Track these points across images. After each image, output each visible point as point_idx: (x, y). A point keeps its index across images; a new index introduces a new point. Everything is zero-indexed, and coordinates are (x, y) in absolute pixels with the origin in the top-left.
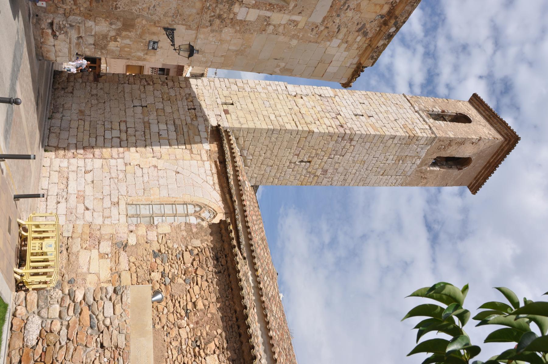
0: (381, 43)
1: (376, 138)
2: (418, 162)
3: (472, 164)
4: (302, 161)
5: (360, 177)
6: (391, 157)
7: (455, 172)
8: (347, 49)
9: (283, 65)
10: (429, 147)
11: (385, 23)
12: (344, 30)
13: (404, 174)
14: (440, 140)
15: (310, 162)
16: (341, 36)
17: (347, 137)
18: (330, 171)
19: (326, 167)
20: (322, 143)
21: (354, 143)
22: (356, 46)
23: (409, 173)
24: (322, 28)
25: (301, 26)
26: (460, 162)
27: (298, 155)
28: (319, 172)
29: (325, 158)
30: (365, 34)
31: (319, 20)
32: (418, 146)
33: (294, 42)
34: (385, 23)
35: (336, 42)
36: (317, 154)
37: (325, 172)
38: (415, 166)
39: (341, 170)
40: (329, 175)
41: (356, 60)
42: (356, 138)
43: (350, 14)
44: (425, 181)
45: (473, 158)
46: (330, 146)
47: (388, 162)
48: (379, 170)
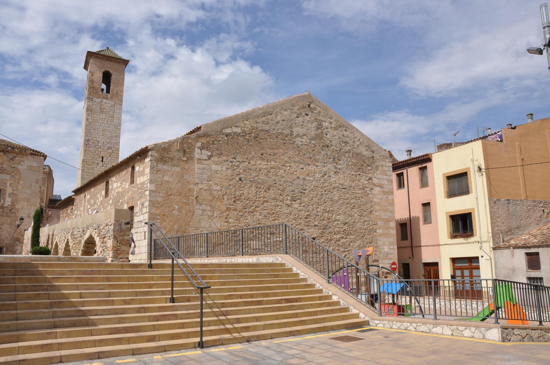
0: (17, 150)
1: (87, 128)
2: (105, 101)
3: (108, 70)
4: (102, 161)
5: (114, 129)
6: (101, 117)
7: (113, 78)
8: (23, 161)
9: (34, 184)
10: (94, 98)
11: (8, 152)
12: (13, 166)
13: (113, 106)
14: (90, 93)
15: (103, 157)
16: (16, 166)
17: (87, 143)
18: (109, 145)
19: (106, 148)
20: (90, 154)
21: (90, 138)
22: (21, 159)
23: (113, 103)
24: (13, 174)
25: (12, 182)
26: (107, 78)
27: (98, 164)
28: (110, 151)
29: (100, 150)
30: (14, 157)
31: (9, 176)
32: (92, 105)
33: (21, 182)
34: (8, 152)
35: (20, 167)
36: (97, 155)
37: (109, 148)
38: (108, 102)
39: (108, 140)
40: (112, 146)
41: (30, 157)
42: (88, 138)
43: (4, 166)
44: (119, 92)
45: (103, 70)
46: (92, 149)
47: (104, 117)
48: (109, 120)
